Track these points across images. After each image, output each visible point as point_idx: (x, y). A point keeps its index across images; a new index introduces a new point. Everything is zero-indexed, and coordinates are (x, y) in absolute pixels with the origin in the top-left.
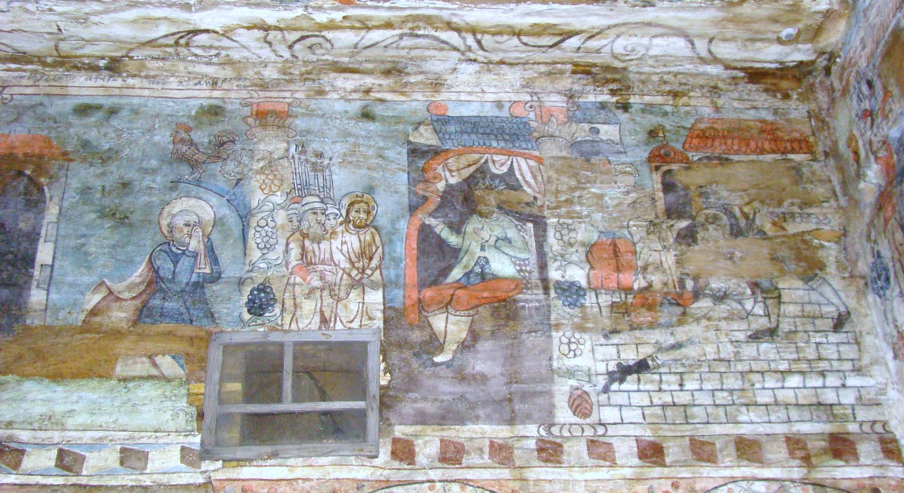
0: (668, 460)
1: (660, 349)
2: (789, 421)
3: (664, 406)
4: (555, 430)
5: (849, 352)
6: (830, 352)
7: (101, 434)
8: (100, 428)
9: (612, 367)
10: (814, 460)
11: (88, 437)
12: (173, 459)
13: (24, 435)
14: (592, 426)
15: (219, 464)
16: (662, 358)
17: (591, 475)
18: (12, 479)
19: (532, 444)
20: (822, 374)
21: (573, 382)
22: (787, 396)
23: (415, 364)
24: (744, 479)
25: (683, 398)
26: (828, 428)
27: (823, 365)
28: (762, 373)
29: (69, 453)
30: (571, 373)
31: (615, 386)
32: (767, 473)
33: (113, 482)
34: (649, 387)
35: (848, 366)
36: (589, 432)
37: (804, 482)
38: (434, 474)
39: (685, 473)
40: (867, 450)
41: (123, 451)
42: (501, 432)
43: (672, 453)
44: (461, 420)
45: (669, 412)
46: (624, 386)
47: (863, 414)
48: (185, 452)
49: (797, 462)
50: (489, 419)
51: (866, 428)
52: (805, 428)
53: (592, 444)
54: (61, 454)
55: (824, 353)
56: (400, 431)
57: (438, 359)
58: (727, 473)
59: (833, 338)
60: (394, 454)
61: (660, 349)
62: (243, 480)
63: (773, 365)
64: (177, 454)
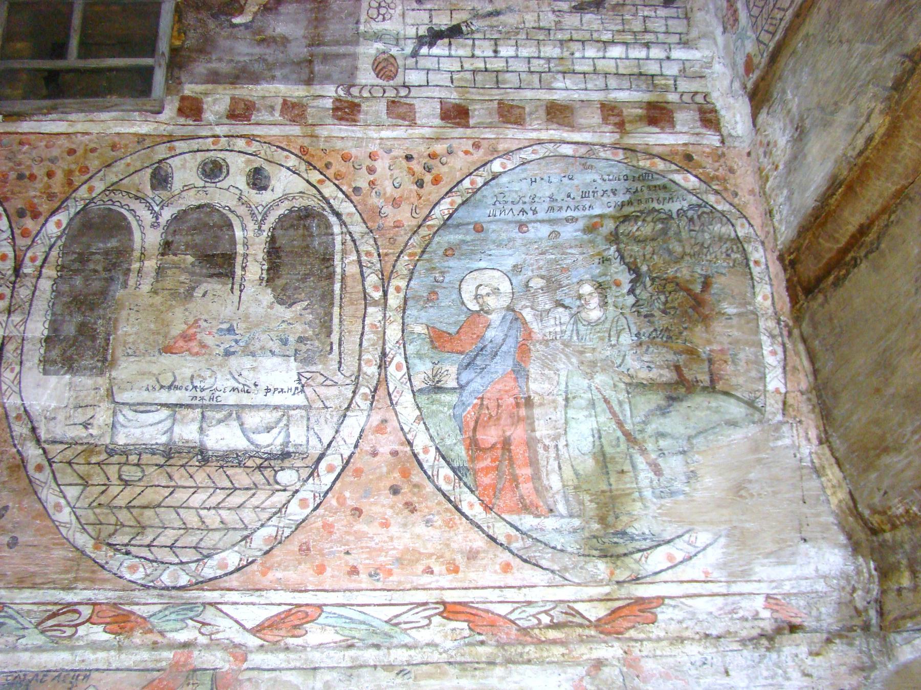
0: (472, 122)
1: (477, 16)
2: (606, 88)
3: (474, 72)
4: (355, 91)
5: (678, 26)
6: (658, 25)
9: (423, 31)
10: (628, 127)
14: (396, 88)
16: (477, 24)
17: (385, 134)
19: (329, 103)
20: (647, 45)
21: (379, 46)
22: (610, 66)
23: (212, 24)
24: (551, 141)
25: (498, 64)
26: (647, 97)
27: (649, 37)
28: (583, 42)
30: (378, 37)
31: (424, 50)
32: (577, 137)
34: (461, 52)
35: (675, 39)
36: (391, 93)
37: (615, 146)
38: (219, 130)
39: (489, 134)
40: (685, 119)
42: (297, 92)
43: (478, 114)
44: (255, 79)
45: (479, 77)
46: (435, 51)
47: (683, 86)
49: (610, 128)
50: (286, 79)
51: (686, 98)
52: (622, 96)
53: (393, 104)
55: (650, 25)
56: (189, 89)
57: (237, 20)
58: (534, 135)
59: (662, 12)
60: (181, 111)
61: (477, 16)
62: (21, 134)
63: (595, 36)
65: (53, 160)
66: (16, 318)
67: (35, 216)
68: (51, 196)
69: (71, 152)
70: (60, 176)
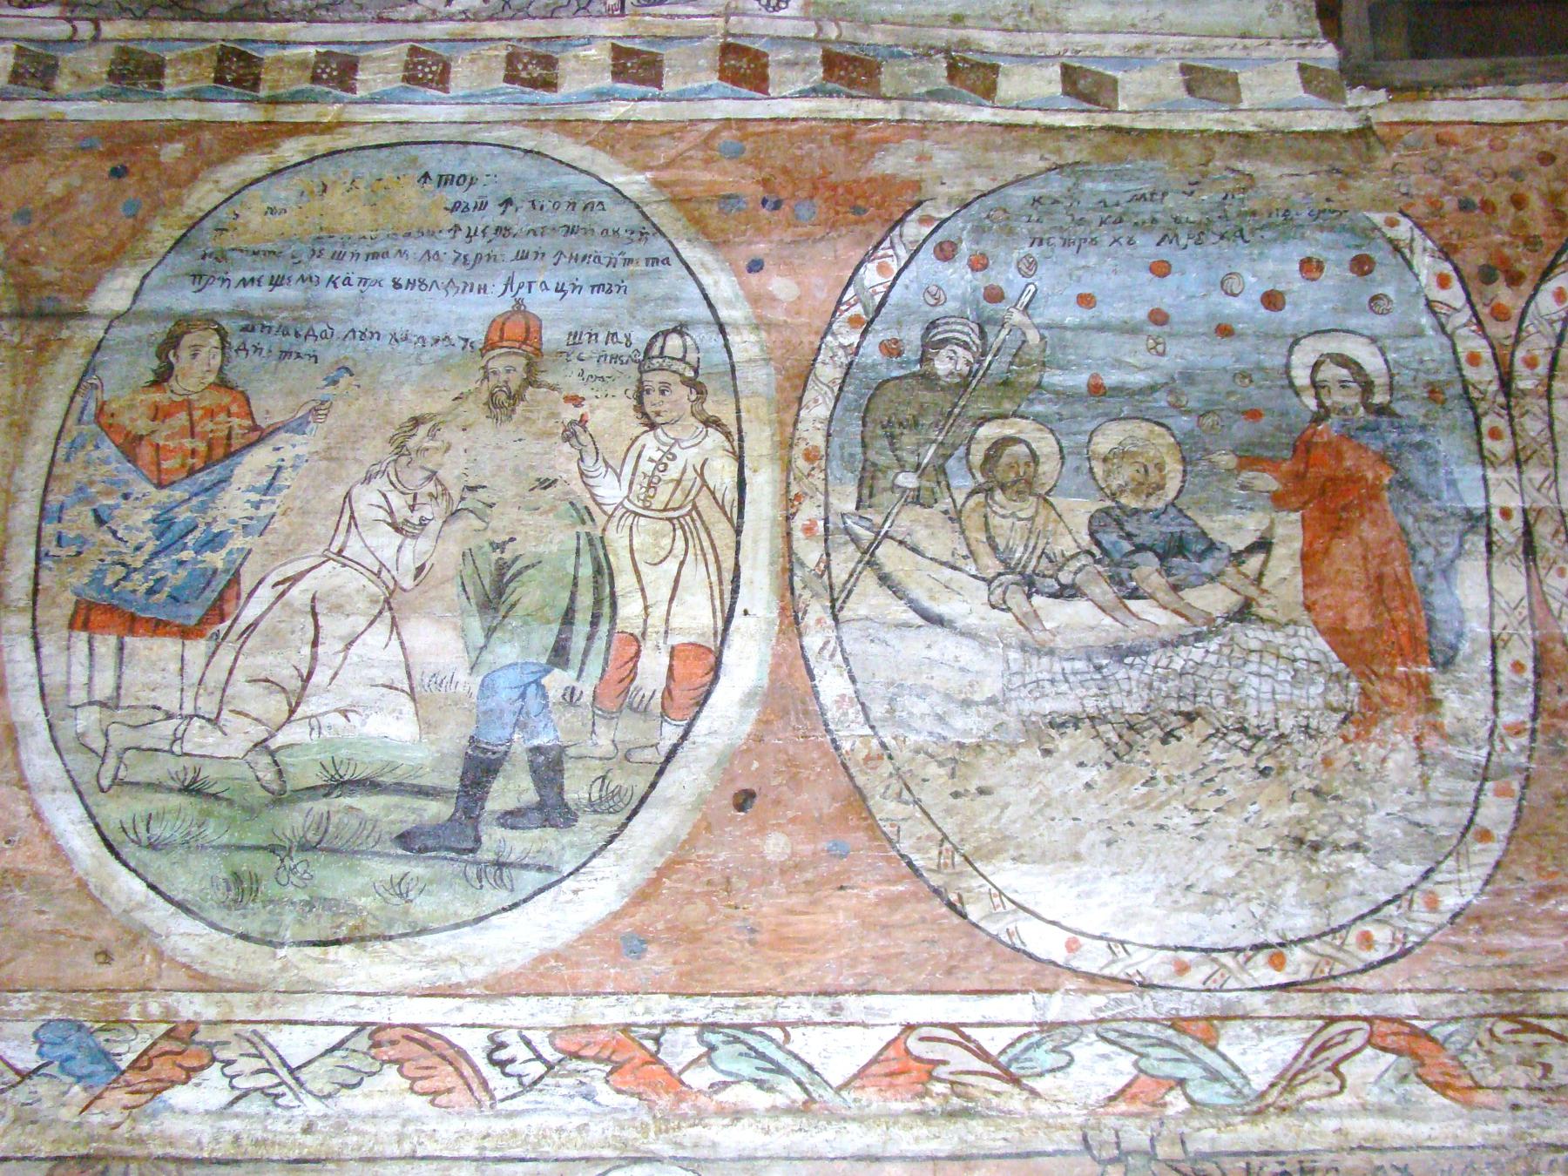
7: (1136, 40)
8: (1133, 28)
11: (1113, 44)
12: (1290, 86)
13: (991, 40)
15: (1381, 95)
18: (986, 114)
29: (1085, 73)
33: (1181, 125)
41: (1186, 70)
48: (1309, 75)
54: (1070, 75)
62: (1436, 124)
64: (1294, 79)
65: (1516, 174)
66: (1535, 474)
67: (1514, 279)
68: (1531, 243)
69: (1547, 159)
70: (1535, 203)
